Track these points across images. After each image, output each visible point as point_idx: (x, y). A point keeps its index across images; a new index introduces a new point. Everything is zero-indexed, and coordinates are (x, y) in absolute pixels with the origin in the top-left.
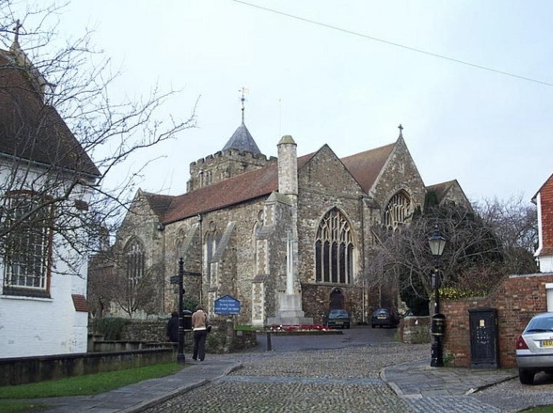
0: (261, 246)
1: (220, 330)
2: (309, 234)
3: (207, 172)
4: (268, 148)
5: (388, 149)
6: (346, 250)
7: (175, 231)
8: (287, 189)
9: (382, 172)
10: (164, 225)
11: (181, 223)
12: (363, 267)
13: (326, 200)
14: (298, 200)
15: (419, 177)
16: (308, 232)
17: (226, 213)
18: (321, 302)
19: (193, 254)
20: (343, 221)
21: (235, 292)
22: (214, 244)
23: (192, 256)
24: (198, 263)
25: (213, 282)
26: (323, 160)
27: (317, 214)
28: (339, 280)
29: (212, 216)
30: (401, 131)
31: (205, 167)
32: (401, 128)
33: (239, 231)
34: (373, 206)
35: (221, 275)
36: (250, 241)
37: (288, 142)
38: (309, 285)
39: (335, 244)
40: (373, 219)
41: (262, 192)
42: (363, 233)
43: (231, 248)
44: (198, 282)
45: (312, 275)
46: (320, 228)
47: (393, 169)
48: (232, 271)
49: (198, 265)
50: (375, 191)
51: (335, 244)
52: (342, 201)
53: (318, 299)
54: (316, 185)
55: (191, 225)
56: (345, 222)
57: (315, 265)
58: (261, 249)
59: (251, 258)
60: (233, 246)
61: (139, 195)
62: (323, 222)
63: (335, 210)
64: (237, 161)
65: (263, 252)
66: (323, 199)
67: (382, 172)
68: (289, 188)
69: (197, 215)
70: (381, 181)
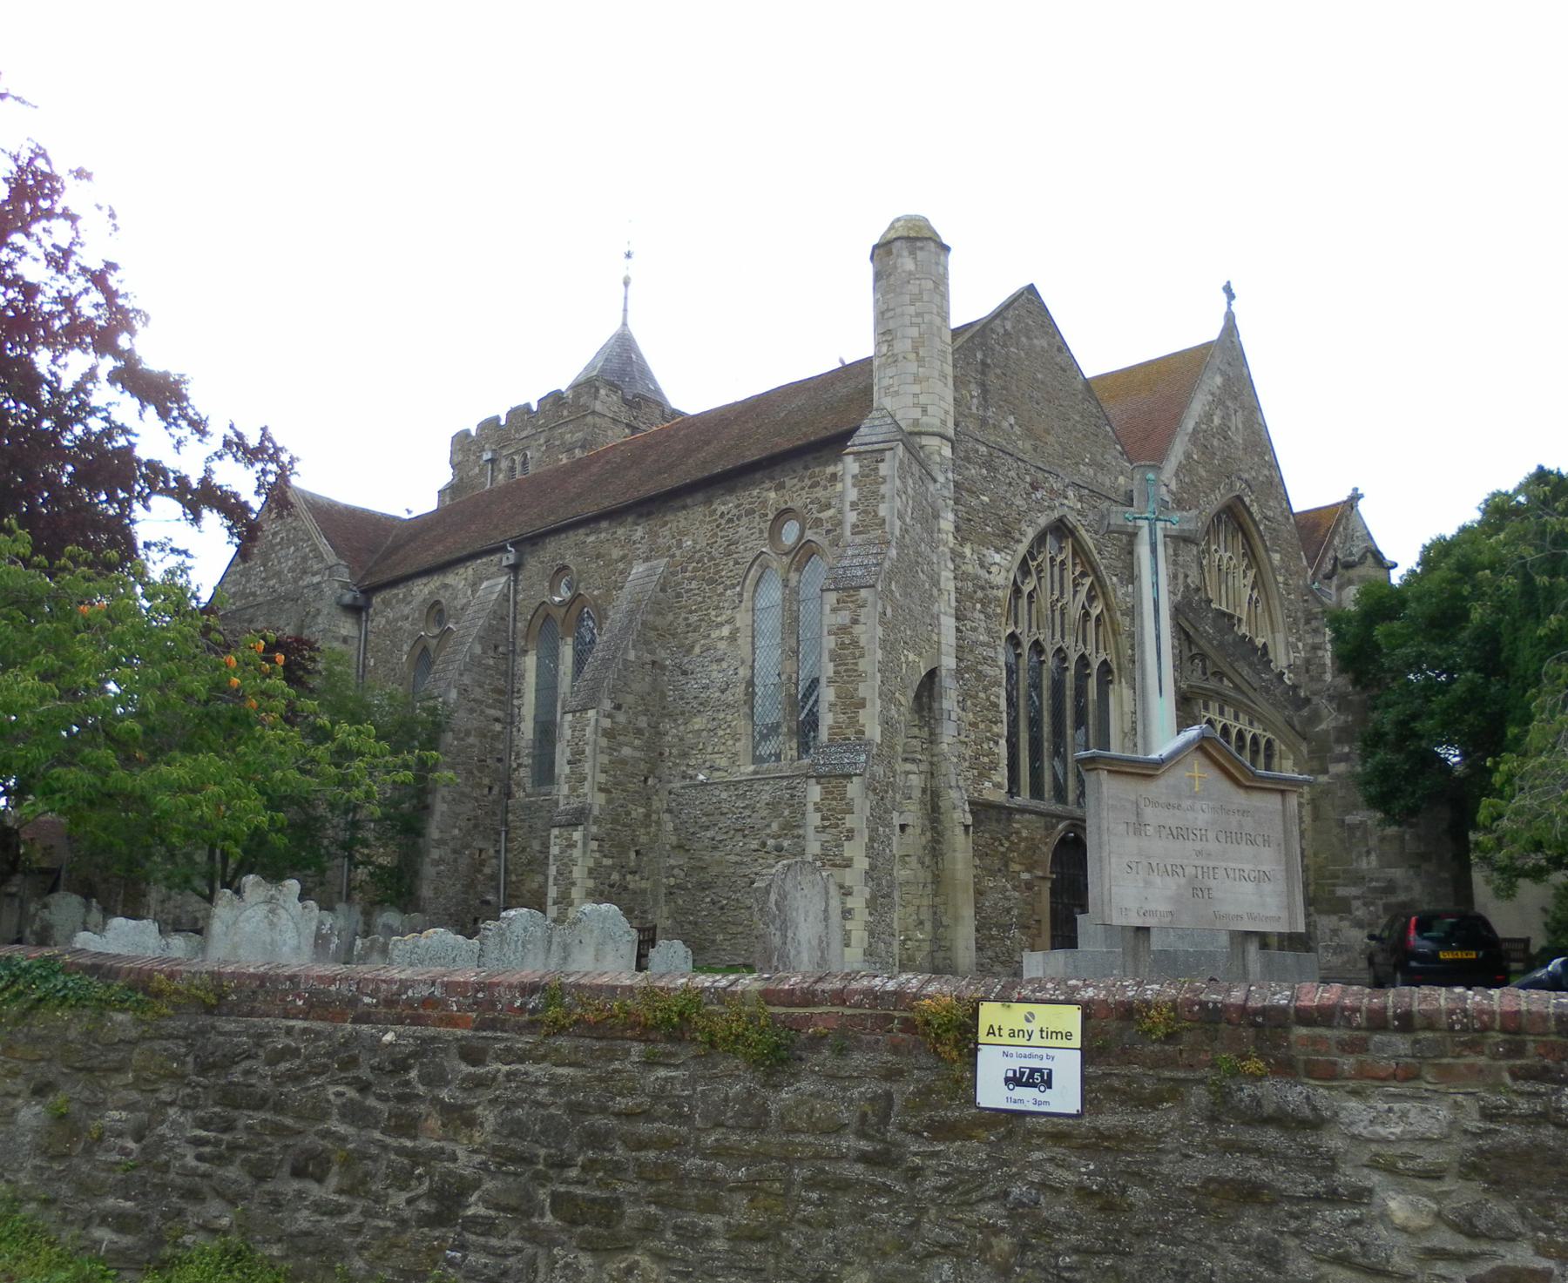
0: (844, 617)
2: (985, 602)
3: (510, 457)
6: (1092, 684)
7: (406, 611)
8: (917, 413)
10: (369, 592)
11: (435, 582)
13: (1035, 487)
15: (1275, 466)
16: (980, 594)
17: (620, 531)
18: (1025, 876)
20: (1083, 575)
23: (477, 693)
24: (497, 720)
25: (573, 789)
26: (1024, 339)
27: (1007, 534)
29: (563, 550)
30: (1229, 304)
32: (1228, 291)
33: (679, 595)
35: (605, 759)
36: (726, 631)
40: (1181, 577)
43: (648, 657)
44: (495, 791)
45: (994, 767)
46: (1017, 591)
47: (1217, 421)
49: (498, 727)
50: (1173, 486)
52: (1080, 500)
53: (1015, 867)
54: (1005, 425)
56: (1088, 581)
57: (1003, 729)
58: (843, 629)
59: (729, 697)
63: (1061, 529)
64: (615, 421)
65: (855, 643)
66: (1028, 479)
68: (925, 411)
69: (503, 549)
70: (1188, 456)
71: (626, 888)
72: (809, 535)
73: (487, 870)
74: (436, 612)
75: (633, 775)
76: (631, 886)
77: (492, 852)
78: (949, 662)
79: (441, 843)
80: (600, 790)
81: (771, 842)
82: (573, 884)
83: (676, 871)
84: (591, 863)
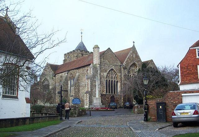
1: (74, 109)
4: (90, 49)
5: (130, 49)
9: (128, 57)
11: (61, 74)
12: (121, 89)
14: (100, 66)
22: (72, 81)
28: (113, 93)
29: (71, 71)
31: (69, 55)
32: (134, 42)
34: (125, 68)
37: (97, 47)
38: (104, 94)
39: (112, 81)
41: (88, 64)
42: (121, 77)
51: (112, 81)
55: (64, 75)
61: (47, 65)
62: (108, 74)
63: (112, 69)
67: (128, 57)
74: (61, 77)
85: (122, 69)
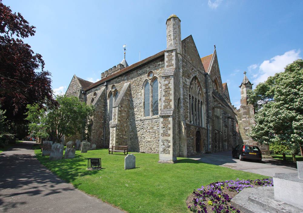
0: (166, 82)
17: (122, 78)
19: (101, 104)
21: (128, 128)
23: (100, 105)
24: (104, 110)
35: (120, 116)
36: (140, 94)
43: (127, 98)
48: (127, 114)
49: (104, 111)
55: (99, 92)
58: (166, 85)
60: (127, 98)
65: (169, 88)
71: (123, 138)
72: (155, 75)
73: (102, 134)
74: (95, 94)
75: (124, 118)
76: (124, 138)
77: (103, 131)
78: (182, 97)
79: (94, 130)
80: (119, 121)
81: (148, 130)
82: (114, 137)
83: (132, 135)
84: (117, 134)
85: (209, 81)
